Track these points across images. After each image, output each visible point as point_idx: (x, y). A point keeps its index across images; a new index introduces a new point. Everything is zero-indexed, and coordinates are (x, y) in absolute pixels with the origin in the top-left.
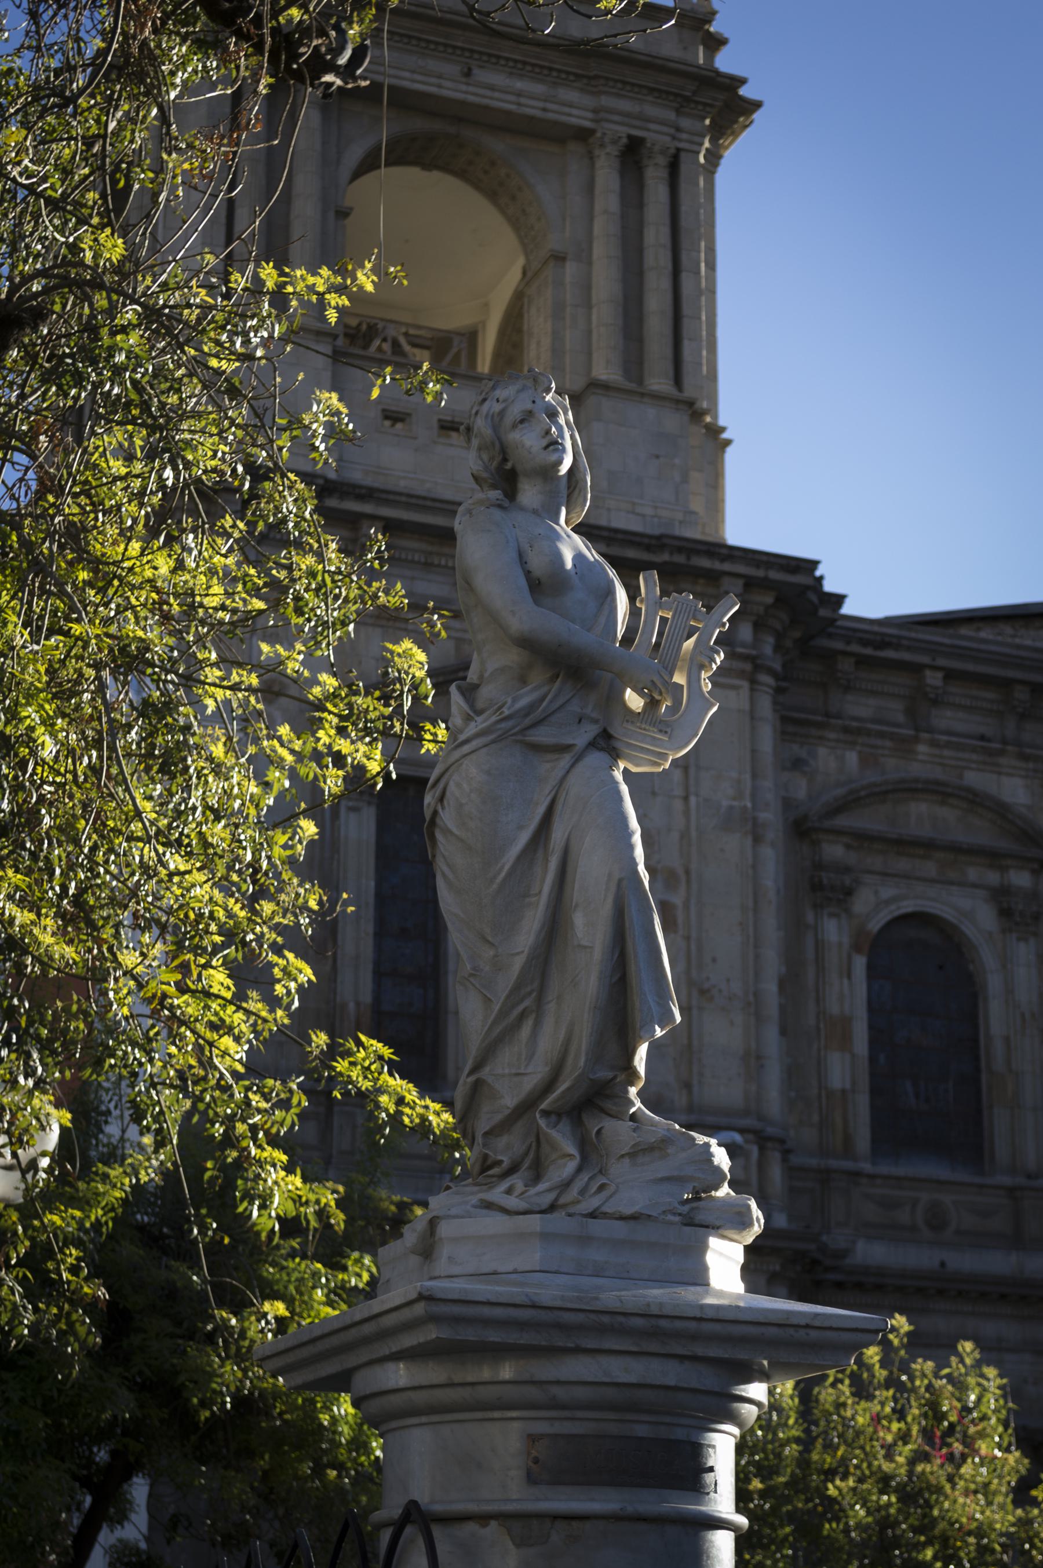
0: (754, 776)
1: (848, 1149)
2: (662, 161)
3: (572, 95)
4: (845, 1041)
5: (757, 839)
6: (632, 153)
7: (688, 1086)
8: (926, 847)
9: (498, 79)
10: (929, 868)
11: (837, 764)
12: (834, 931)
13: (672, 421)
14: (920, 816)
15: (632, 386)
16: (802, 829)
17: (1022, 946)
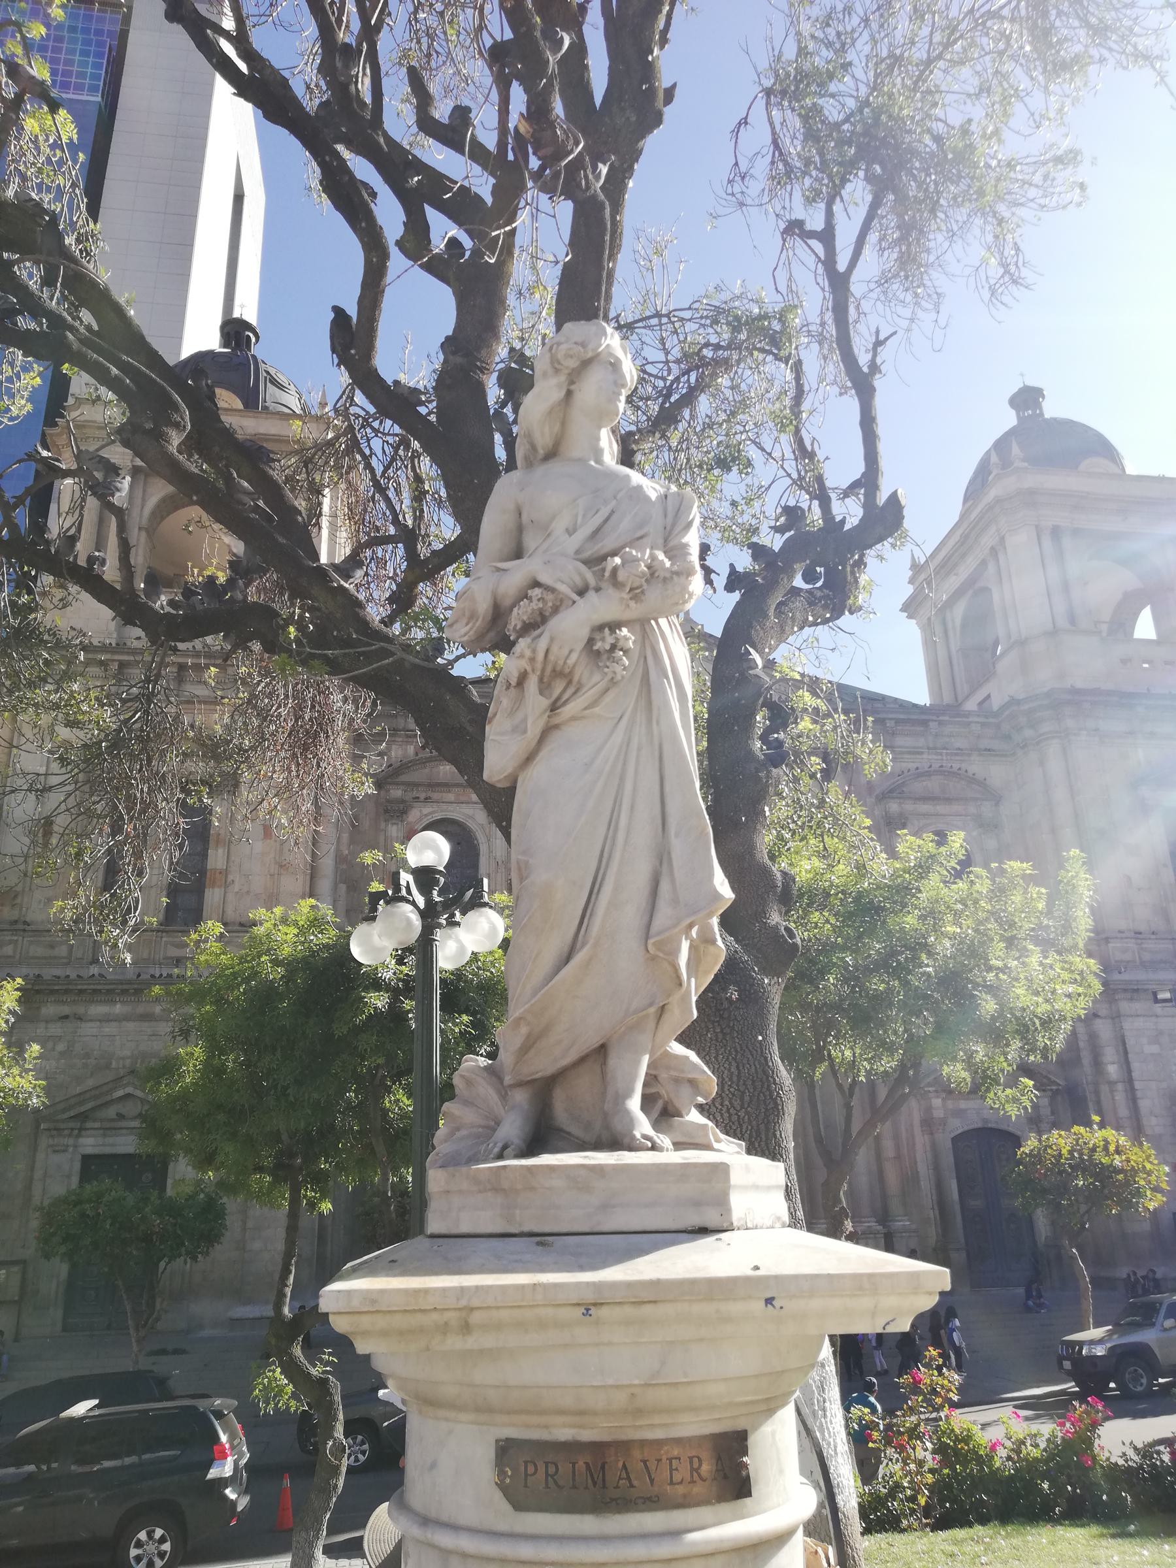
17: (395, 827)
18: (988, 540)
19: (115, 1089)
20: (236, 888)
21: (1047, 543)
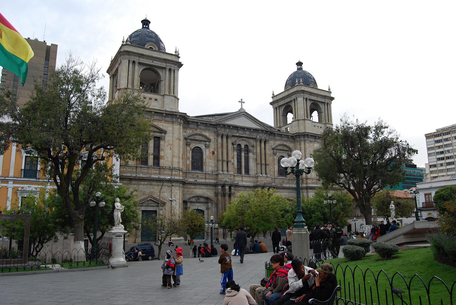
0: (180, 134)
1: (189, 170)
2: (173, 71)
3: (164, 64)
4: (189, 159)
5: (180, 141)
6: (170, 70)
7: (172, 165)
8: (197, 140)
9: (156, 62)
10: (198, 142)
11: (189, 132)
13: (173, 98)
14: (197, 137)
15: (169, 95)
16: (185, 139)
18: (293, 97)
19: (147, 199)
20: (166, 159)
21: (305, 101)
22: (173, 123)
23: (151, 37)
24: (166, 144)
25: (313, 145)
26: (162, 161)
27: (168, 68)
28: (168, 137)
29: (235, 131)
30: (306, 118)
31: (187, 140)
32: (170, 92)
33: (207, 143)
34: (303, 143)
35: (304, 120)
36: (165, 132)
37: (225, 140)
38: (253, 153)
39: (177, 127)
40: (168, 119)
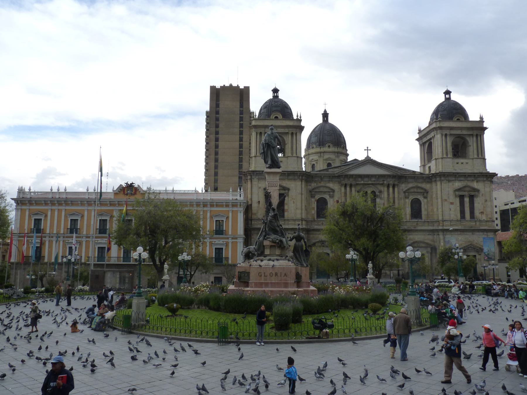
6: (292, 134)
8: (322, 192)
12: (313, 200)
13: (296, 158)
14: (322, 189)
16: (310, 191)
22: (295, 180)
23: (276, 106)
24: (290, 199)
25: (453, 185)
26: (286, 214)
27: (290, 132)
28: (291, 193)
29: (360, 179)
30: (445, 156)
31: (312, 193)
32: (292, 153)
33: (332, 193)
34: (439, 183)
35: (442, 158)
36: (289, 189)
37: (348, 189)
38: (381, 198)
39: (299, 183)
40: (290, 177)
